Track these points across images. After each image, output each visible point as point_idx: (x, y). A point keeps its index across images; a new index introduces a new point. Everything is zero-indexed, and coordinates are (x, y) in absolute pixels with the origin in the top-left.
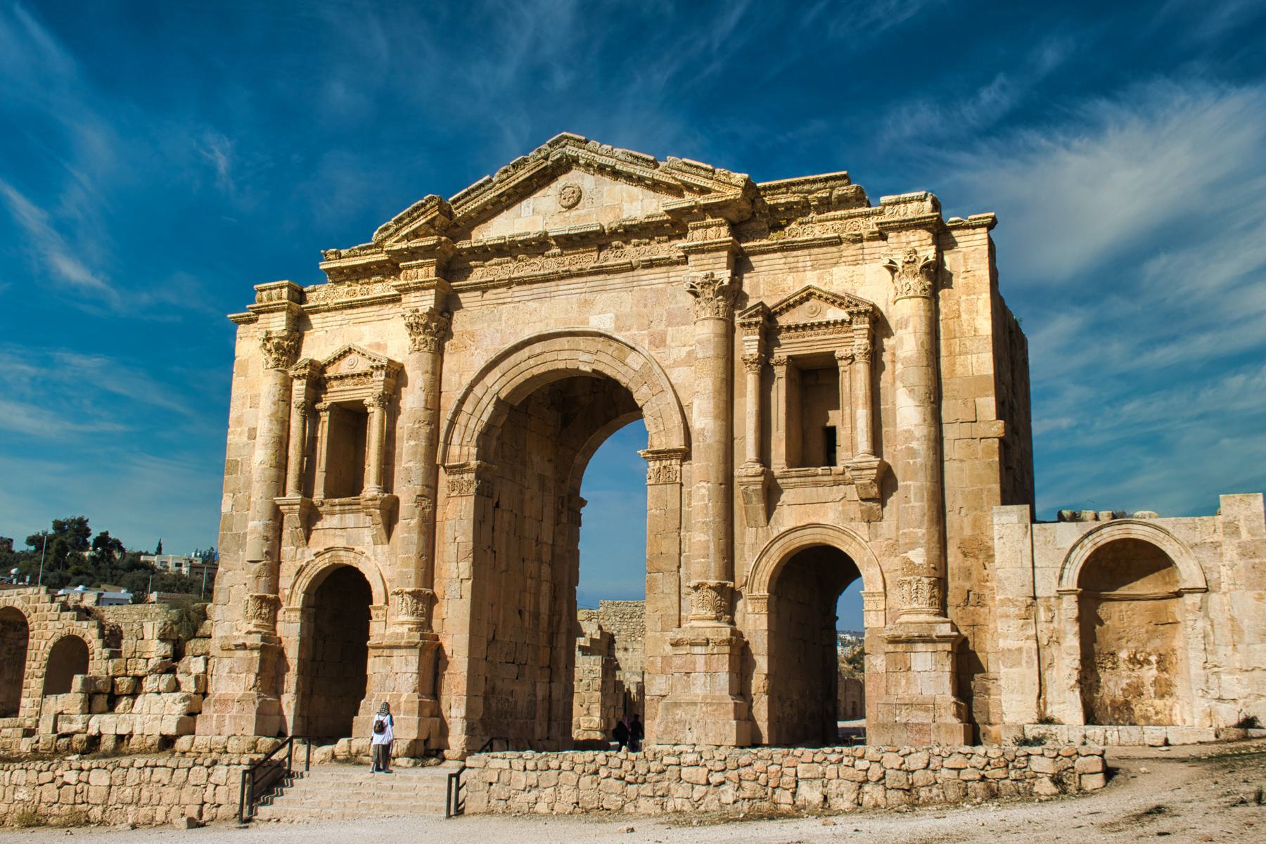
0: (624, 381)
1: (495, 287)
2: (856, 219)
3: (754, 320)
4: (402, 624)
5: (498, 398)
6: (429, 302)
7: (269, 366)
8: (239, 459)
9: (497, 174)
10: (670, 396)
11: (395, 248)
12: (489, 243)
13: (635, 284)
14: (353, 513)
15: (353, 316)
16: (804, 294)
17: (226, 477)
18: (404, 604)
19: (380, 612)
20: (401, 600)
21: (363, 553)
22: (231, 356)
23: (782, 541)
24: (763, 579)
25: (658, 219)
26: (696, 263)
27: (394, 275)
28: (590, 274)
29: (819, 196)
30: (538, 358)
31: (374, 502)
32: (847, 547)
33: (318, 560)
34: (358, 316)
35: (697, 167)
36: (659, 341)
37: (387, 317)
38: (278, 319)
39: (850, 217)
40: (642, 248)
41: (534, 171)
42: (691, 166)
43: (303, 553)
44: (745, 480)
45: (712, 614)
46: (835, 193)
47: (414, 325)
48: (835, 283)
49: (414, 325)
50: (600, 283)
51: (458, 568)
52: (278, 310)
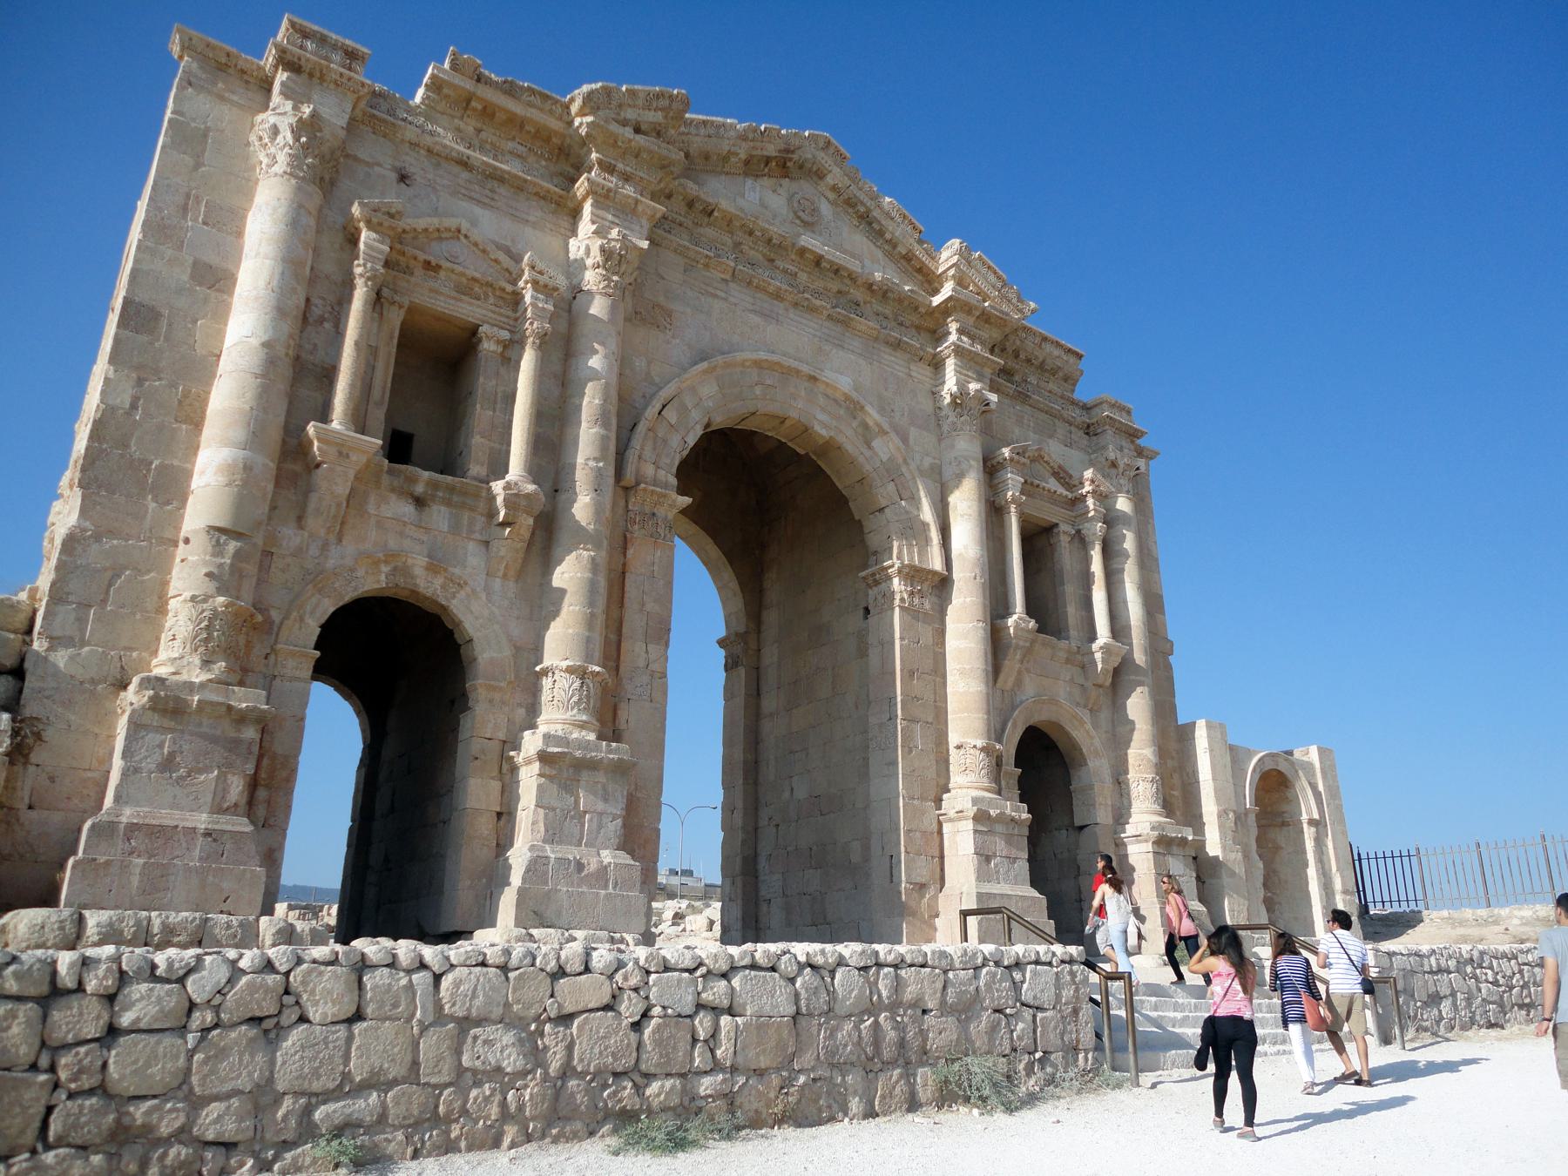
0: (868, 467)
4: (582, 726)
20: (577, 684)
27: (546, 160)
35: (989, 267)
51: (647, 652)
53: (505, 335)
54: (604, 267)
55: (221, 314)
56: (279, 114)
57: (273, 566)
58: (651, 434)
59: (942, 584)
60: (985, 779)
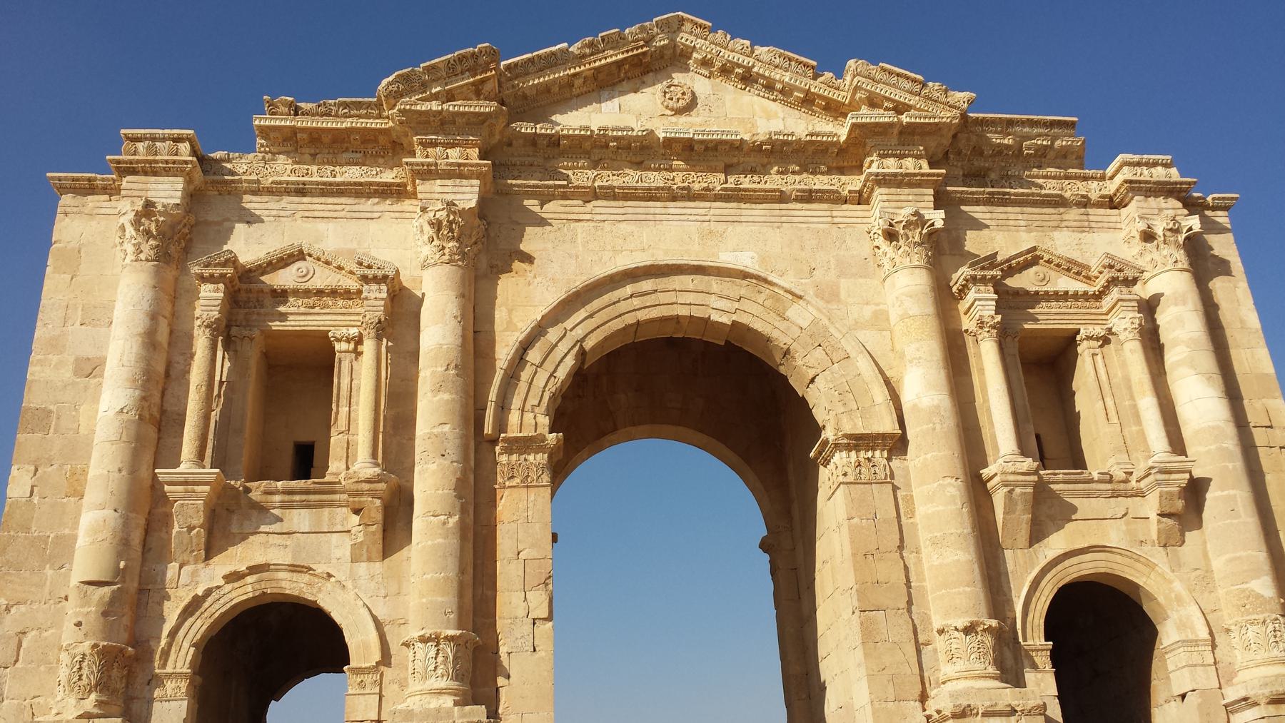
1: (564, 197)
2: (1074, 181)
3: (989, 273)
4: (440, 692)
5: (582, 349)
6: (469, 196)
7: (142, 256)
8: (51, 407)
9: (578, 44)
10: (864, 365)
11: (418, 108)
12: (565, 132)
13: (784, 219)
14: (308, 507)
15: (302, 207)
16: (1029, 256)
17: (21, 437)
18: (440, 659)
19: (368, 679)
20: (433, 653)
21: (330, 576)
22: (43, 242)
23: (1054, 571)
24: (1036, 621)
25: (825, 139)
26: (890, 197)
27: (383, 157)
28: (718, 198)
29: (1039, 142)
30: (645, 298)
31: (373, 486)
32: (1144, 579)
33: (228, 587)
34: (310, 207)
35: (898, 75)
36: (830, 295)
37: (369, 215)
38: (166, 186)
39: (1067, 177)
40: (791, 178)
41: (630, 54)
42: (891, 73)
43: (194, 574)
44: (1012, 478)
45: (991, 670)
46: (1058, 143)
47: (445, 223)
48: (1059, 249)
49: (445, 223)
50: (732, 212)
52: (167, 172)
53: (354, 331)
54: (438, 238)
55: (96, 399)
56: (124, 214)
57: (150, 601)
58: (514, 381)
59: (898, 444)
60: (978, 667)
